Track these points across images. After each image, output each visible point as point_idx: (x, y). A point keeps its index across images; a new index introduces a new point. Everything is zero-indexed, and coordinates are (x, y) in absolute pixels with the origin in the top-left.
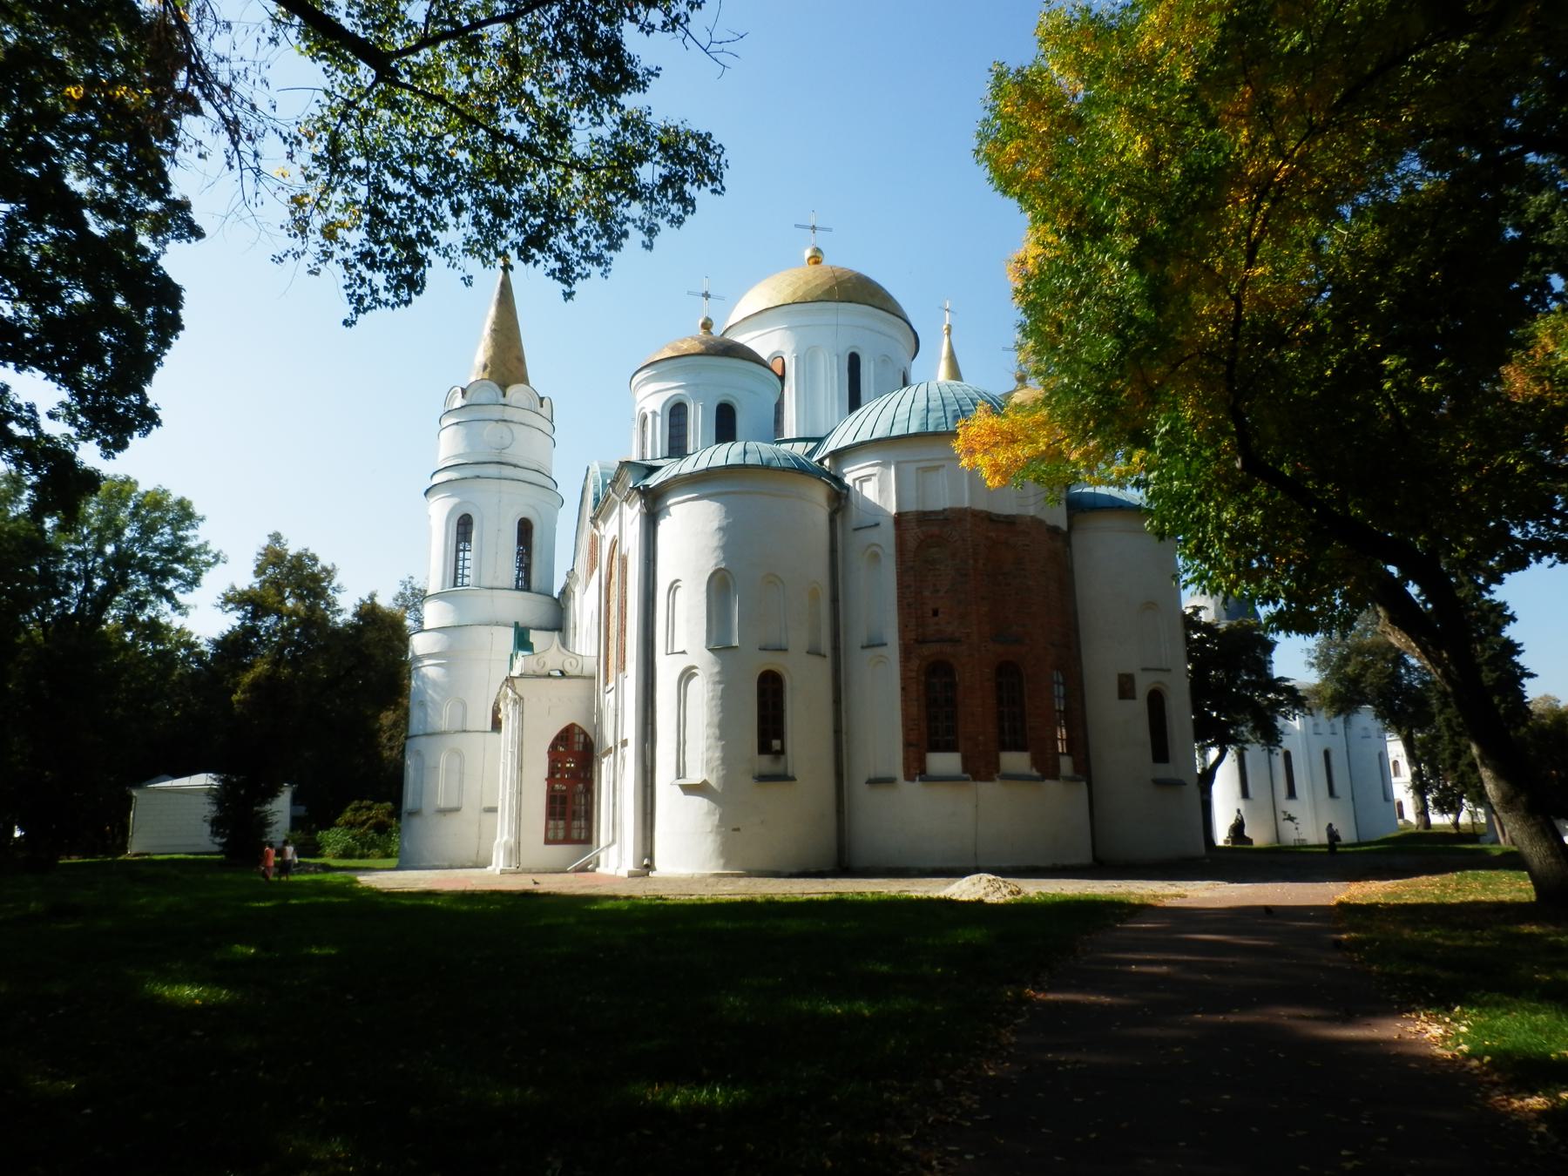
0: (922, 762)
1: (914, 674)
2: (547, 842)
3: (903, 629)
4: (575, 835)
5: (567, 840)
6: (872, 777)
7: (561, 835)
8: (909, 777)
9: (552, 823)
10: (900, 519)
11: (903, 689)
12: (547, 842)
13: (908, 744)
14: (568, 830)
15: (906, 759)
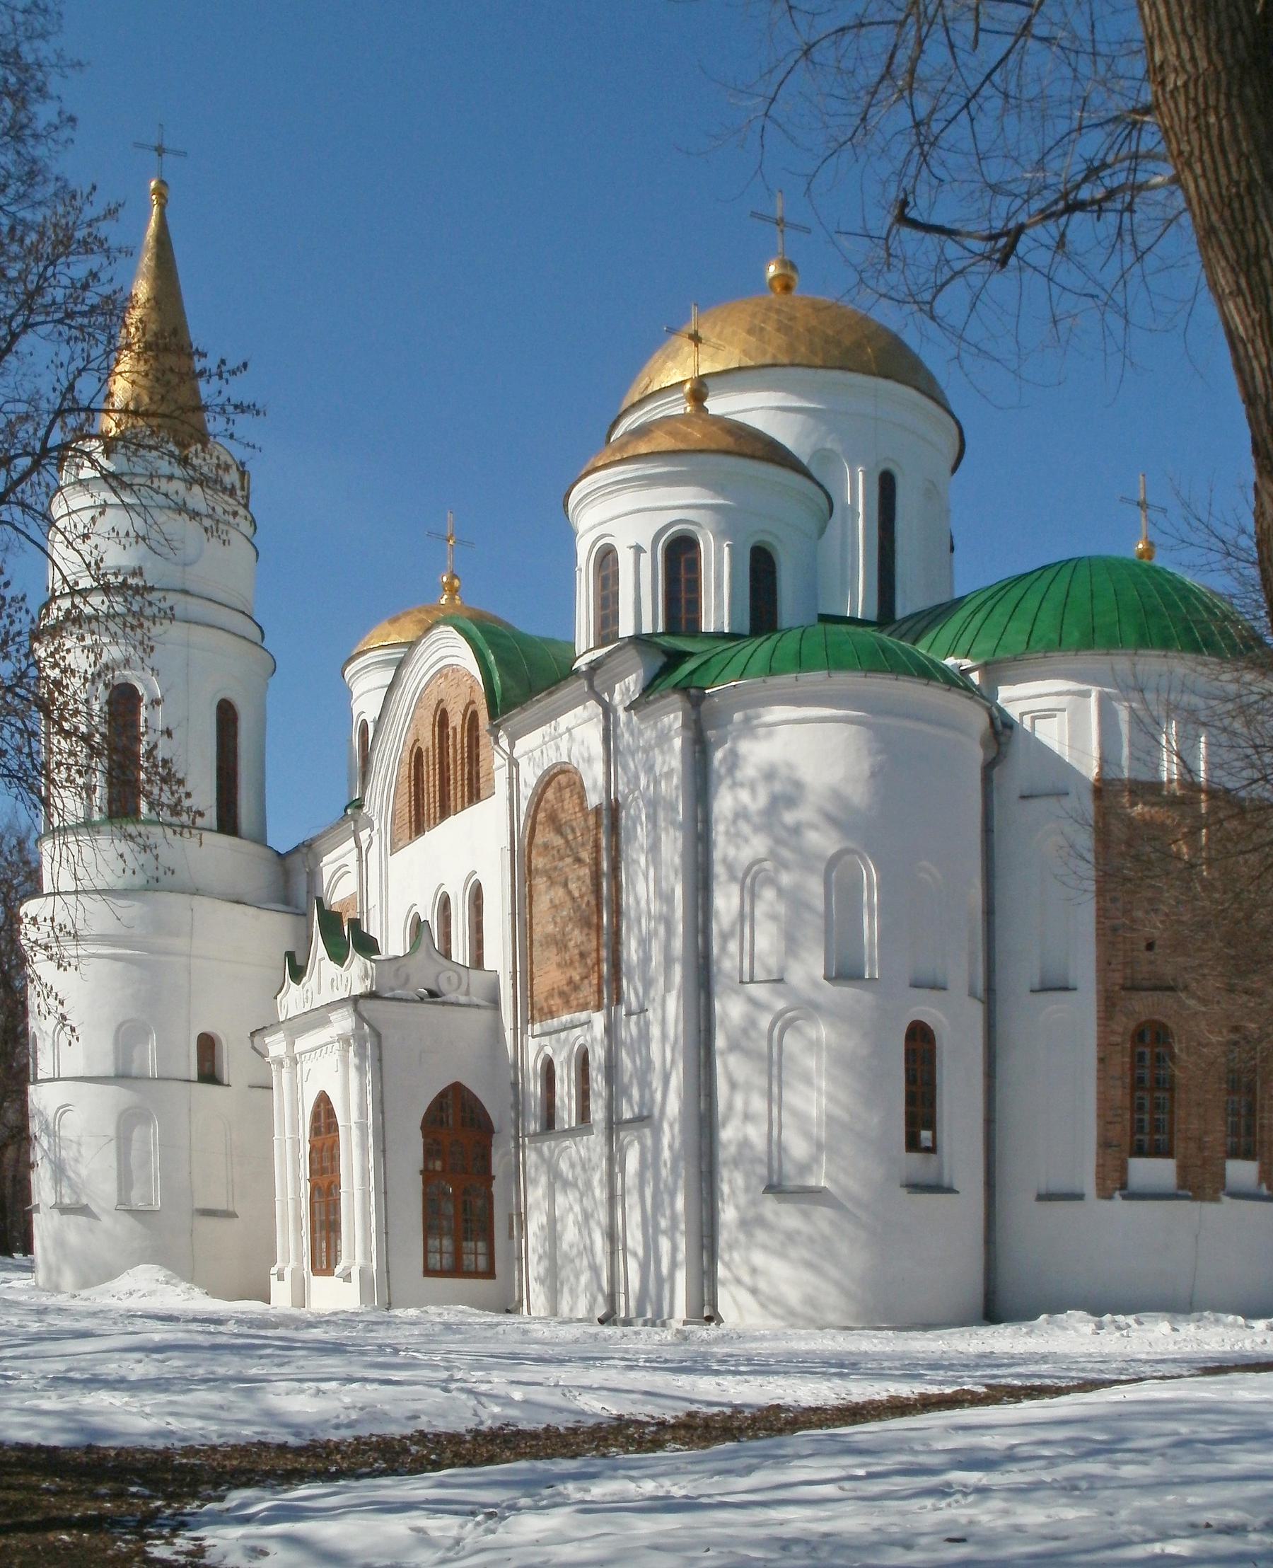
0: (1123, 1169)
1: (1118, 1039)
2: (428, 1272)
3: (1104, 966)
4: (468, 1260)
5: (457, 1270)
6: (1043, 1191)
7: (447, 1261)
8: (1105, 1194)
9: (433, 1243)
10: (1102, 789)
11: (1101, 1060)
12: (428, 1272)
13: (1105, 1144)
14: (458, 1254)
15: (1101, 1167)
